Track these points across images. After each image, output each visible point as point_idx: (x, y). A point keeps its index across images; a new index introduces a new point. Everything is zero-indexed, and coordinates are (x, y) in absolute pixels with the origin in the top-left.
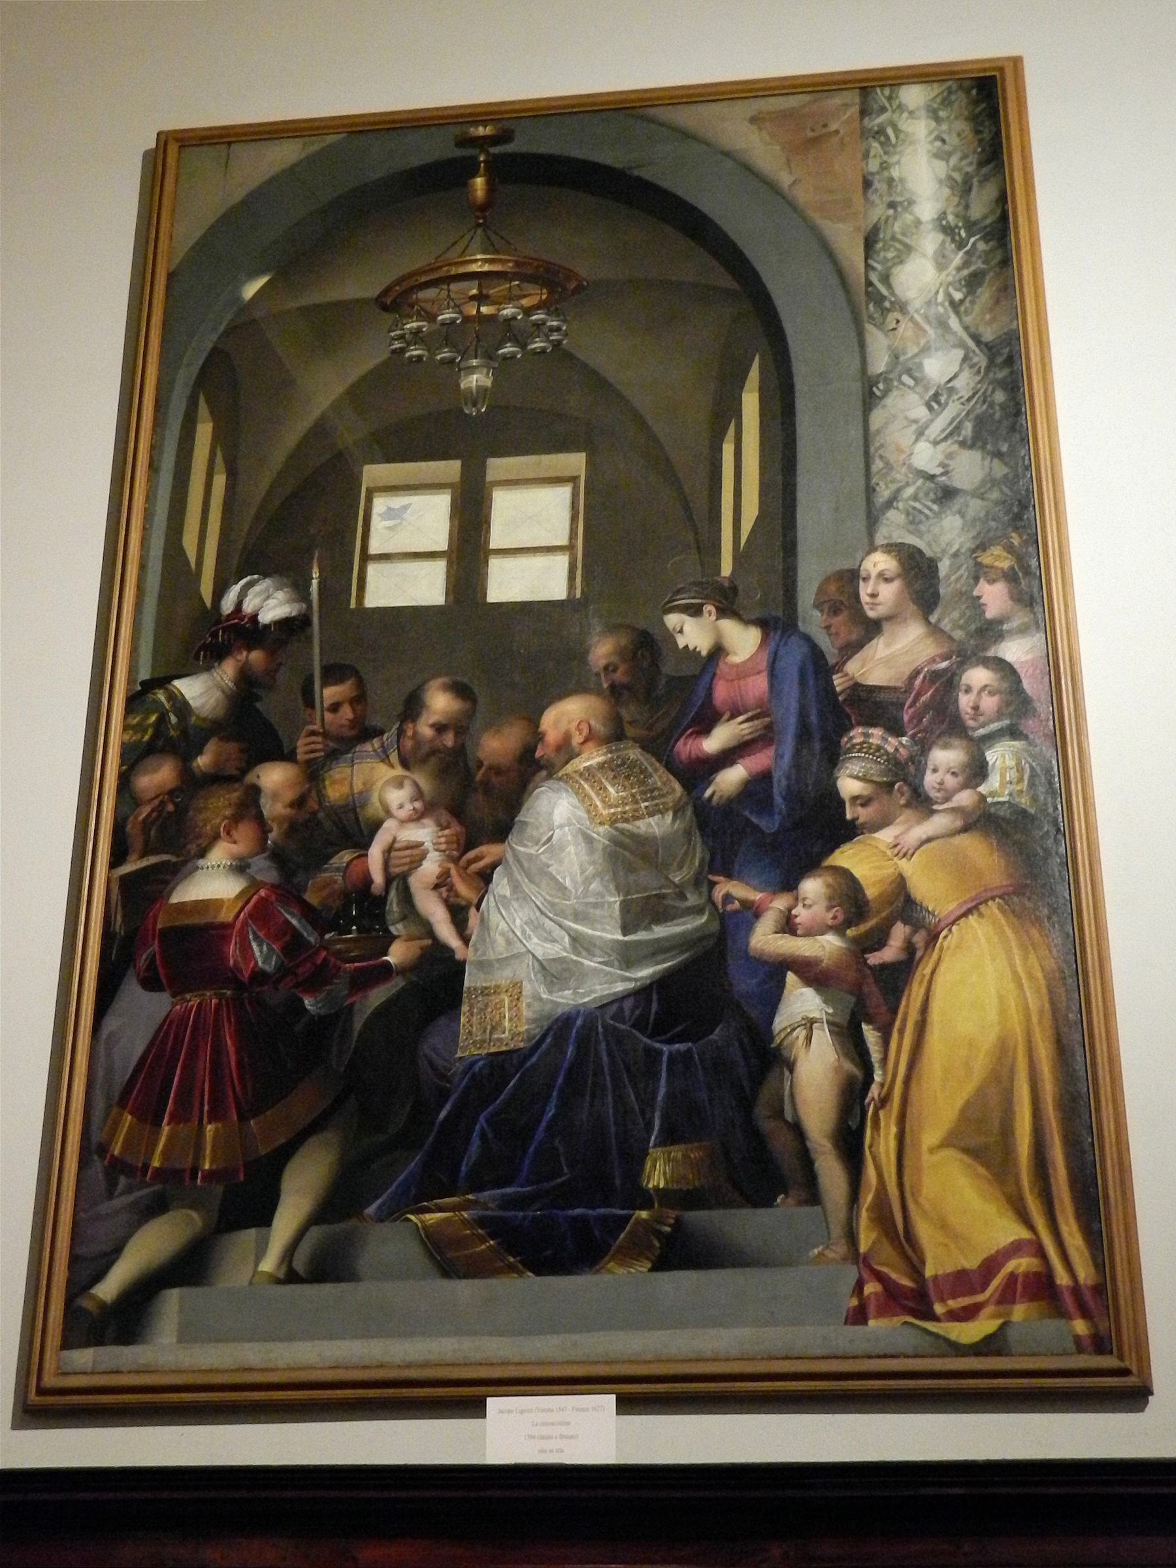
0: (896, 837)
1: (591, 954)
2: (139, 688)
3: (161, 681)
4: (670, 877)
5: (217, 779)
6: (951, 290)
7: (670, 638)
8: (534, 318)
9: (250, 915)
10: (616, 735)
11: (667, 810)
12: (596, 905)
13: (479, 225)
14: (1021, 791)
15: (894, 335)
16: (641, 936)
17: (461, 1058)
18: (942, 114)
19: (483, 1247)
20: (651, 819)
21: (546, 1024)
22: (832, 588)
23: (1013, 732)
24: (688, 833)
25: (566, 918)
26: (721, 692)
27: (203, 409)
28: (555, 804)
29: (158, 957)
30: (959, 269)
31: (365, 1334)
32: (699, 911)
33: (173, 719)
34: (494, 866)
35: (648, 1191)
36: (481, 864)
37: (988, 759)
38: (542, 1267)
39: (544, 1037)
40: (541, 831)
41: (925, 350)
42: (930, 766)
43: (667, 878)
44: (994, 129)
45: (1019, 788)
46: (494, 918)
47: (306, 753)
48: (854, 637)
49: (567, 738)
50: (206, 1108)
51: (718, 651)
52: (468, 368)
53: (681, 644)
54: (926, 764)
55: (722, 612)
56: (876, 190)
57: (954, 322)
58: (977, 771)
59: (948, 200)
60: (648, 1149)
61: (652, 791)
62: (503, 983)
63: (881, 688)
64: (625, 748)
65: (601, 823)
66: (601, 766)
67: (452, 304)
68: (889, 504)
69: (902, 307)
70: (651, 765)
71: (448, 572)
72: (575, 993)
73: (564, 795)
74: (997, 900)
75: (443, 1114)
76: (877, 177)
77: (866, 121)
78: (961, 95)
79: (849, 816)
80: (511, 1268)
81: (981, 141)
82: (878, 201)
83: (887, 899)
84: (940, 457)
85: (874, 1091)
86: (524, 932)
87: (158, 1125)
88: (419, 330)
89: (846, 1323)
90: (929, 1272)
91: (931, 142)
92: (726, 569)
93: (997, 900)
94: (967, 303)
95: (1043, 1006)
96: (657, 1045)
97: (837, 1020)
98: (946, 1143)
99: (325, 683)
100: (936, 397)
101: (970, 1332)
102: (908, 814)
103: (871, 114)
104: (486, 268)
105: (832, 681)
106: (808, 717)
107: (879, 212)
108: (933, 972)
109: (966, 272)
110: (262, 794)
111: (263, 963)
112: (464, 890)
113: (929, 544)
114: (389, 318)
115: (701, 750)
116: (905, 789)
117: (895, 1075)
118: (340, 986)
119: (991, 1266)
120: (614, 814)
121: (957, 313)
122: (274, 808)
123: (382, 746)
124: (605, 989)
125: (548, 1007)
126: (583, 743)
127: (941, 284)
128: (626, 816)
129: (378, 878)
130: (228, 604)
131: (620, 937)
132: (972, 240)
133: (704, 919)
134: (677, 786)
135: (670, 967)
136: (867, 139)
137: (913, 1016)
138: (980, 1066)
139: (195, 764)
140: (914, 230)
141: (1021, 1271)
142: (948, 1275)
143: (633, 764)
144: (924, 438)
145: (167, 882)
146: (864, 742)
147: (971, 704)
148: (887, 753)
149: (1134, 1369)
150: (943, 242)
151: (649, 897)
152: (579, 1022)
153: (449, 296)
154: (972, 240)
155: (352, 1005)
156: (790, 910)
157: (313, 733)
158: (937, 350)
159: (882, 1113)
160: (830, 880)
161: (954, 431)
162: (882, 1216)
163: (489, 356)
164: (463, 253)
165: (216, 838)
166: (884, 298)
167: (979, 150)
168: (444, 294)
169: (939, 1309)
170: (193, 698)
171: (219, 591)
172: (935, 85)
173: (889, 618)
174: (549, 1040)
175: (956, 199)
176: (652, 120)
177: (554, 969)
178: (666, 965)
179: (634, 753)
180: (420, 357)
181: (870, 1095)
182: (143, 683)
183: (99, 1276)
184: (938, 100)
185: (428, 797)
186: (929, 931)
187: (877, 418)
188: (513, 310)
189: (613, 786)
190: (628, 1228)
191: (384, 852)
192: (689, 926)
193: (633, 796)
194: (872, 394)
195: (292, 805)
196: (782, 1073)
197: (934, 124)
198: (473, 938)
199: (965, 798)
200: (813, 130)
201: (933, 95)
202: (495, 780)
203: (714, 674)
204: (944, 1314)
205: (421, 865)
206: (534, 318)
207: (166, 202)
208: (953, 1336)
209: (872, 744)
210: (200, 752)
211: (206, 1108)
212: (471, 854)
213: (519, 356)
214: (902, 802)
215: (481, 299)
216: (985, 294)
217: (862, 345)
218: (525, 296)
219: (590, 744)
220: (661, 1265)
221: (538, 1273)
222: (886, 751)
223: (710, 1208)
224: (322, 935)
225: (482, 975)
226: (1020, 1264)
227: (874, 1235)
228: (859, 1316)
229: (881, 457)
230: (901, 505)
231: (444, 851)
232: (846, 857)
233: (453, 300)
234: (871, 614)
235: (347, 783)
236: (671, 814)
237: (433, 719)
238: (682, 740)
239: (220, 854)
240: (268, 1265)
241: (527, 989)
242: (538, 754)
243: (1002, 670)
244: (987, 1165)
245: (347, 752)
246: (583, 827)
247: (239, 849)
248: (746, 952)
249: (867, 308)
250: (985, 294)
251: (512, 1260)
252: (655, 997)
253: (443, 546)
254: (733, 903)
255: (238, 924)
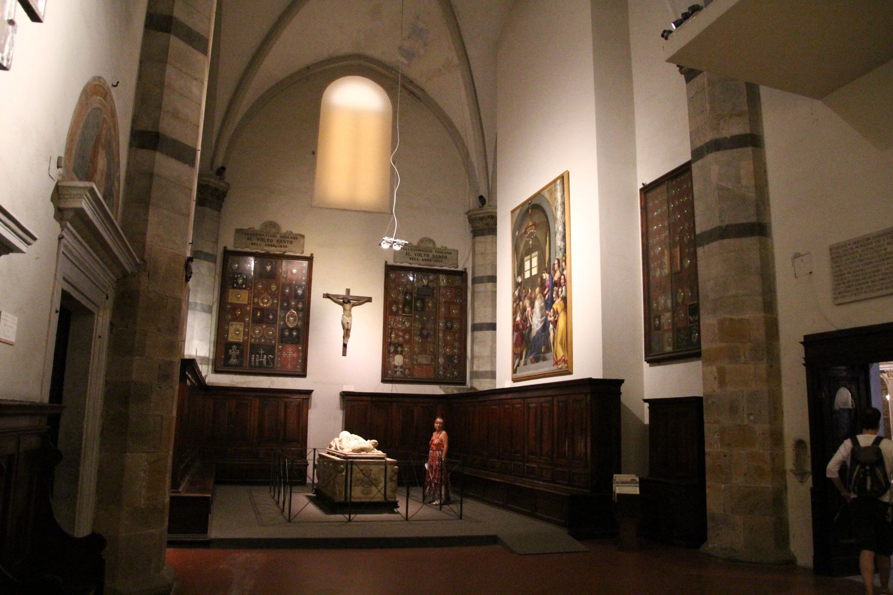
101: (560, 367)
122: (521, 308)
239: (518, 315)
240: (523, 364)
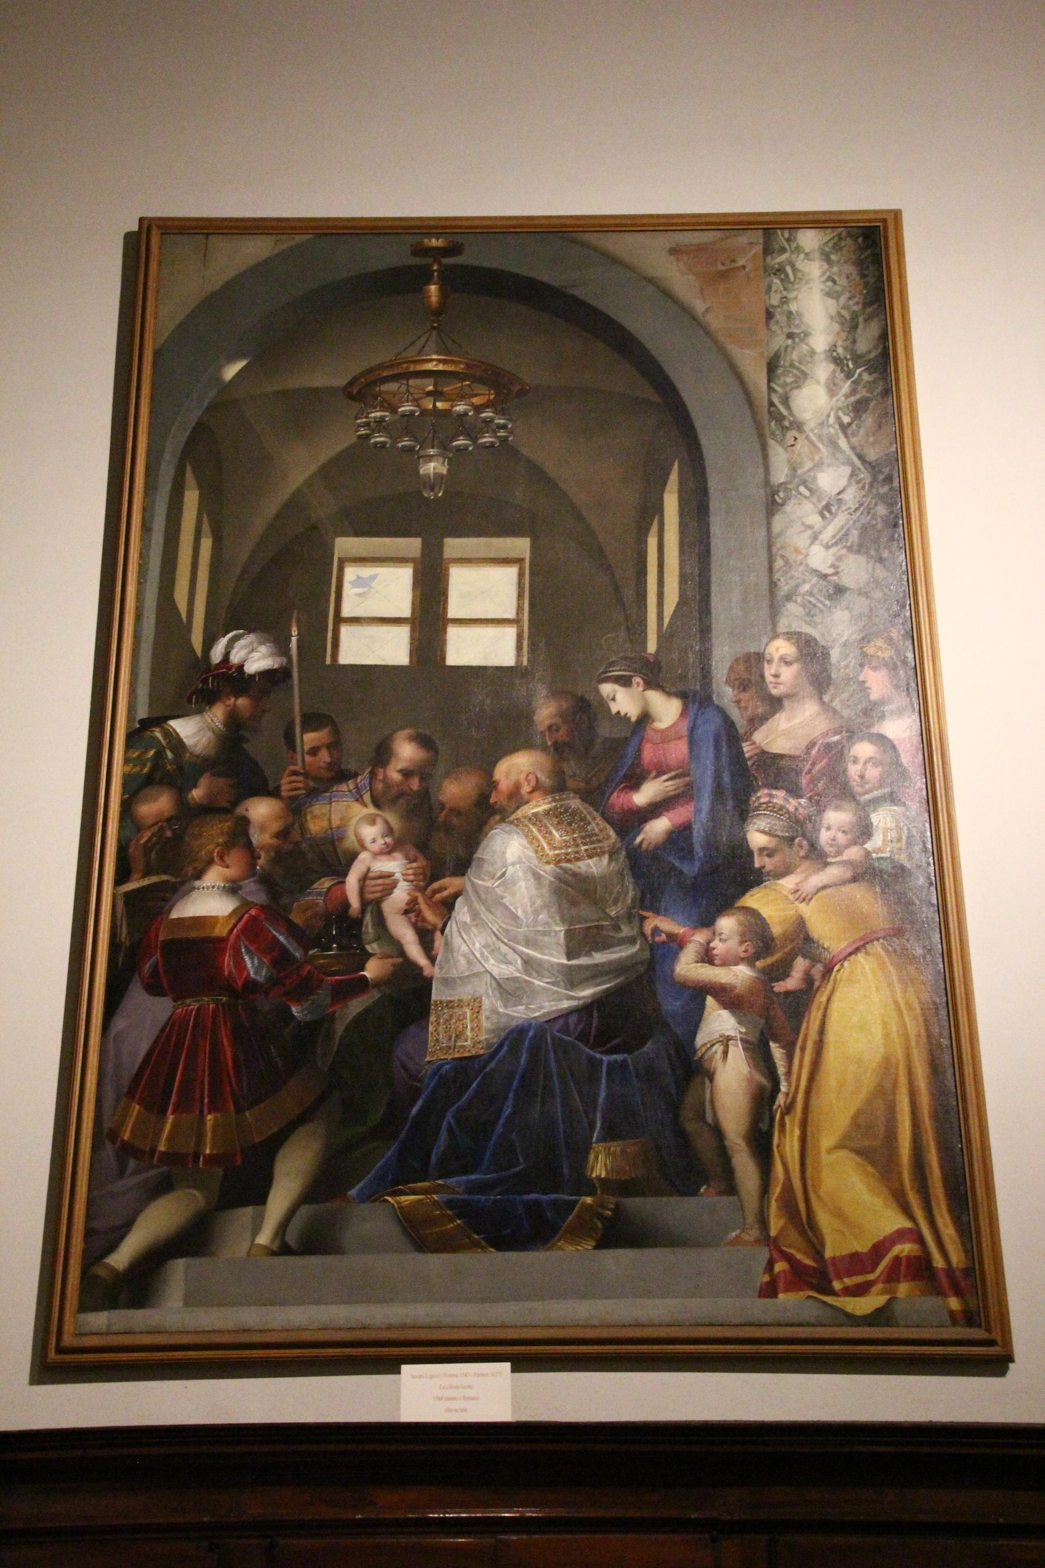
0: (797, 884)
1: (540, 975)
2: (138, 726)
3: (158, 720)
4: (607, 910)
5: (208, 810)
6: (840, 413)
7: (603, 705)
8: (483, 415)
9: (243, 931)
10: (559, 787)
11: (603, 853)
12: (544, 933)
13: (434, 328)
14: (900, 849)
15: (792, 450)
16: (583, 961)
17: (429, 1062)
18: (833, 257)
19: (452, 1225)
20: (590, 861)
21: (503, 1035)
22: (741, 667)
23: (892, 798)
24: (621, 874)
25: (518, 943)
26: (648, 754)
27: (189, 477)
28: (509, 843)
29: (160, 965)
30: (847, 396)
31: (348, 1301)
32: (632, 941)
33: (170, 755)
34: (456, 896)
35: (592, 1180)
36: (445, 893)
37: (873, 820)
38: (503, 1242)
39: (501, 1046)
40: (496, 866)
41: (818, 466)
42: (825, 823)
43: (606, 913)
44: (877, 274)
45: (898, 846)
46: (457, 941)
47: (289, 791)
48: (760, 710)
49: (517, 787)
50: (206, 1100)
51: (645, 718)
52: (426, 456)
53: (614, 710)
54: (821, 823)
55: (649, 685)
56: (777, 322)
57: (843, 443)
58: (864, 831)
59: (838, 334)
60: (591, 1143)
61: (590, 836)
62: (466, 997)
63: (782, 756)
64: (568, 798)
65: (548, 863)
66: (547, 813)
67: (410, 398)
68: (789, 597)
69: (799, 426)
70: (590, 813)
71: (412, 638)
72: (527, 1008)
73: (515, 837)
74: (881, 940)
75: (415, 1110)
76: (779, 310)
77: (769, 258)
78: (849, 241)
79: (757, 865)
80: (474, 1245)
81: (866, 284)
82: (779, 332)
83: (788, 937)
84: (831, 559)
85: (781, 1100)
86: (482, 954)
87: (163, 1112)
88: (382, 418)
89: (760, 1296)
90: (828, 1254)
91: (824, 282)
92: (652, 647)
93: (881, 940)
94: (854, 426)
95: (919, 1031)
96: (598, 1056)
97: (749, 1038)
98: (840, 1146)
99: (305, 729)
100: (827, 507)
101: (863, 1305)
102: (806, 864)
103: (773, 252)
104: (441, 367)
105: (741, 748)
106: (722, 778)
107: (779, 341)
108: (829, 1000)
109: (853, 399)
110: (251, 826)
111: (256, 973)
112: (430, 916)
113: (823, 635)
114: (355, 406)
115: (630, 801)
116: (805, 843)
117: (797, 1087)
118: (323, 996)
119: (879, 1249)
120: (558, 855)
121: (846, 436)
123: (357, 787)
124: (552, 1006)
125: (504, 1020)
126: (531, 792)
127: (832, 409)
128: (568, 857)
129: (355, 902)
130: (217, 654)
131: (565, 961)
132: (858, 371)
133: (637, 947)
134: (612, 833)
135: (608, 988)
136: (769, 275)
137: (813, 1035)
138: (868, 1082)
139: (190, 796)
140: (809, 359)
141: (904, 1254)
142: (843, 1257)
143: (574, 813)
144: (817, 542)
145: (165, 900)
146: (769, 802)
147: (858, 773)
148: (788, 812)
149: (999, 1340)
150: (834, 371)
151: (589, 927)
152: (531, 1033)
153: (408, 391)
154: (858, 371)
155: (334, 1012)
156: (708, 943)
157: (295, 773)
158: (829, 466)
159: (787, 1119)
160: (742, 918)
161: (841, 538)
162: (788, 1204)
163: (445, 447)
164: (420, 353)
165: (210, 862)
166: (784, 418)
167: (865, 291)
168: (404, 388)
169: (837, 1285)
170: (186, 737)
171: (209, 643)
172: (829, 231)
173: (790, 696)
174: (505, 1048)
175: (845, 334)
176: (584, 245)
177: (509, 987)
178: (604, 987)
179: (575, 803)
180: (383, 444)
181: (777, 1103)
182: (141, 721)
183: (112, 1247)
184: (830, 245)
185: (397, 834)
186: (825, 967)
187: (778, 522)
188: (465, 407)
189: (558, 830)
190: (575, 1211)
191: (359, 881)
192: (623, 954)
193: (574, 839)
194: (774, 502)
195: (277, 835)
196: (703, 1083)
197: (826, 266)
198: (439, 958)
199: (853, 853)
200: (723, 264)
201: (828, 238)
202: (455, 821)
203: (643, 738)
204: (841, 1290)
205: (390, 894)
206: (483, 415)
207: (152, 284)
208: (849, 1309)
209: (776, 804)
210: (195, 786)
211: (206, 1100)
212: (436, 885)
213: (470, 449)
214: (802, 853)
215: (436, 395)
216: (869, 419)
217: (765, 457)
218: (476, 395)
219: (536, 794)
220: (605, 1243)
221: (499, 1249)
222: (787, 810)
223: (644, 1195)
224: (306, 951)
225: (447, 992)
226: (903, 1250)
227: (781, 1222)
228: (770, 1290)
229: (782, 556)
230: (799, 599)
231: (412, 881)
232: (753, 900)
233: (412, 394)
234: (775, 692)
235: (325, 818)
236: (607, 856)
237: (401, 765)
238: (615, 794)
239: (214, 876)
240: (264, 1238)
241: (486, 1003)
242: (492, 800)
243: (883, 745)
244: (873, 1163)
245: (326, 791)
246: (532, 866)
247: (232, 872)
248: (672, 979)
249: (770, 426)
250: (869, 419)
251: (476, 1237)
252: (595, 1014)
253: (406, 612)
254: (660, 935)
255: (232, 937)
